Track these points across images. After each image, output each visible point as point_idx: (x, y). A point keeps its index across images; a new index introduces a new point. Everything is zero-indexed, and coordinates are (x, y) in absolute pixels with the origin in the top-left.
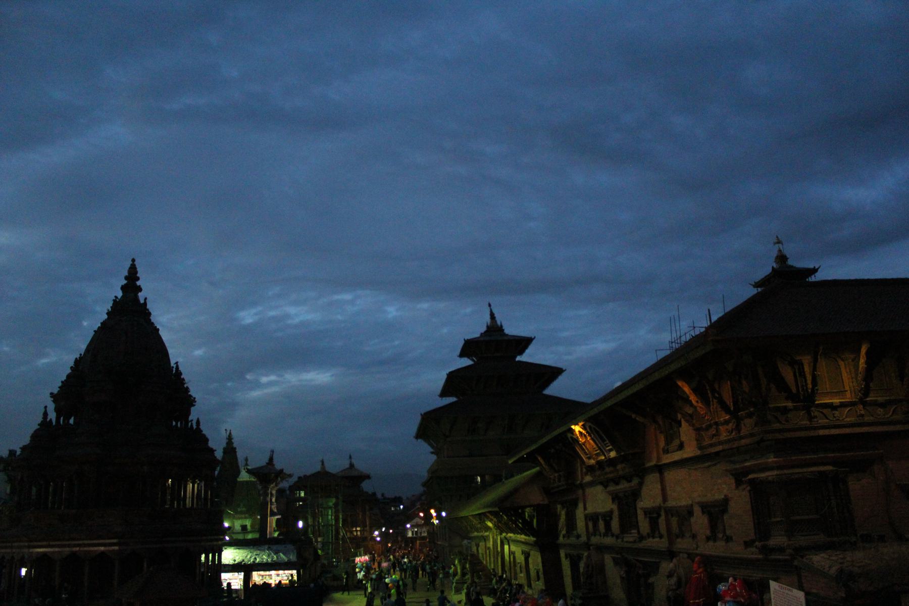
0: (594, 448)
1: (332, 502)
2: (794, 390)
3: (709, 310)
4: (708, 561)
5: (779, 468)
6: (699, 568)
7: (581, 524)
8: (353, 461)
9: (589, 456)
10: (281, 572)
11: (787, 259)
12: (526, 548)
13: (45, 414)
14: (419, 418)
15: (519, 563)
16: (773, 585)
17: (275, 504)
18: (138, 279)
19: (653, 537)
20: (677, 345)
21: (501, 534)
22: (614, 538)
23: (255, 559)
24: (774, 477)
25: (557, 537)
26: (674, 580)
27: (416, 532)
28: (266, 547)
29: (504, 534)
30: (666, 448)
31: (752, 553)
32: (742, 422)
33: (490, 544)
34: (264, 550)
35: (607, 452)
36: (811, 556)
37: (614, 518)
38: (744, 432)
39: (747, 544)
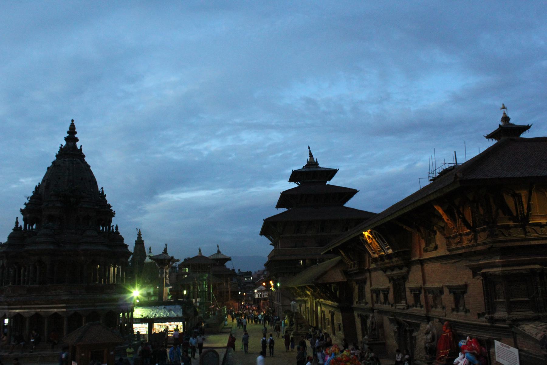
0: (378, 247)
2: (515, 214)
3: (455, 152)
4: (452, 325)
5: (503, 266)
6: (447, 329)
7: (368, 295)
9: (373, 251)
10: (172, 323)
11: (510, 119)
12: (332, 309)
13: (17, 223)
14: (263, 222)
15: (327, 319)
16: (497, 343)
17: (168, 279)
18: (76, 133)
19: (416, 307)
20: (433, 175)
21: (316, 299)
22: (390, 306)
23: (156, 315)
24: (499, 272)
25: (352, 303)
26: (429, 336)
27: (260, 294)
28: (163, 307)
29: (317, 300)
30: (426, 248)
31: (483, 321)
32: (478, 234)
33: (309, 305)
34: (161, 309)
36: (523, 326)
38: (480, 241)
39: (479, 315)
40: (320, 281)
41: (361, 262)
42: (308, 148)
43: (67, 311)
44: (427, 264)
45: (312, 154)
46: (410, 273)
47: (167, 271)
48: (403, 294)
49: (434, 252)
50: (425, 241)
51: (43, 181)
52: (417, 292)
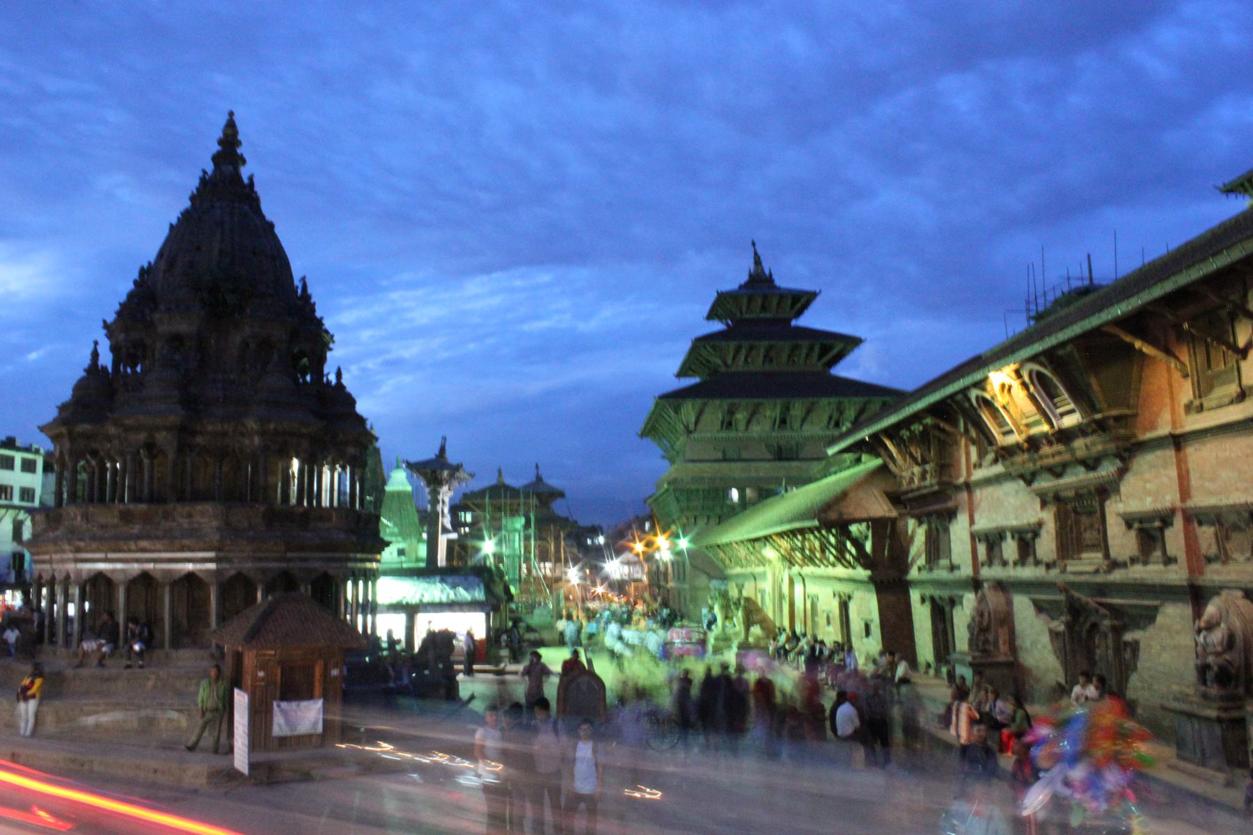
1: (519, 522)
8: (541, 472)
13: (95, 355)
19: (1146, 563)
21: (790, 568)
23: (423, 596)
28: (438, 578)
29: (796, 569)
30: (1197, 403)
33: (767, 586)
34: (435, 583)
35: (1055, 416)
37: (1043, 533)
40: (833, 515)
41: (945, 466)
42: (751, 243)
43: (217, 572)
45: (759, 258)
47: (447, 500)
48: (1089, 536)
50: (1193, 384)
51: (161, 255)
52: (1157, 524)
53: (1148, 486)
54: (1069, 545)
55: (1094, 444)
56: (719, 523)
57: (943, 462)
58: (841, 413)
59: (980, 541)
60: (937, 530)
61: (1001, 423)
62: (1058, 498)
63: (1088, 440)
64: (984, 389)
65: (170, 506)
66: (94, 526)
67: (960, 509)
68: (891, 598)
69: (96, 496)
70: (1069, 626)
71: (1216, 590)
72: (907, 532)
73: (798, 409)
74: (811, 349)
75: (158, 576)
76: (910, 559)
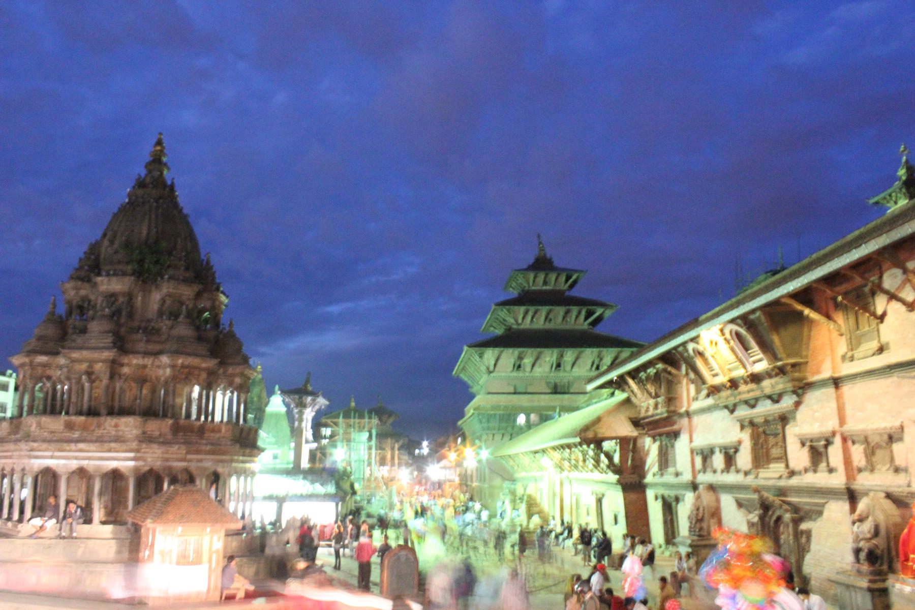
0: (727, 361)
9: (713, 372)
21: (561, 473)
25: (643, 475)
28: (301, 476)
29: (565, 473)
30: (850, 354)
35: (749, 364)
40: (590, 435)
41: (671, 400)
44: (850, 386)
46: (802, 408)
48: (775, 452)
49: (874, 357)
50: (847, 341)
53: (816, 414)
54: (761, 458)
55: (777, 383)
56: (511, 439)
57: (671, 396)
58: (601, 359)
59: (697, 454)
60: (666, 444)
61: (711, 369)
62: (752, 424)
63: (773, 380)
64: (697, 343)
65: (102, 419)
66: (45, 432)
67: (682, 431)
68: (633, 496)
69: (49, 409)
70: (762, 518)
71: (866, 494)
72: (644, 446)
73: (569, 355)
74: (579, 313)
75: (91, 470)
76: (646, 468)
